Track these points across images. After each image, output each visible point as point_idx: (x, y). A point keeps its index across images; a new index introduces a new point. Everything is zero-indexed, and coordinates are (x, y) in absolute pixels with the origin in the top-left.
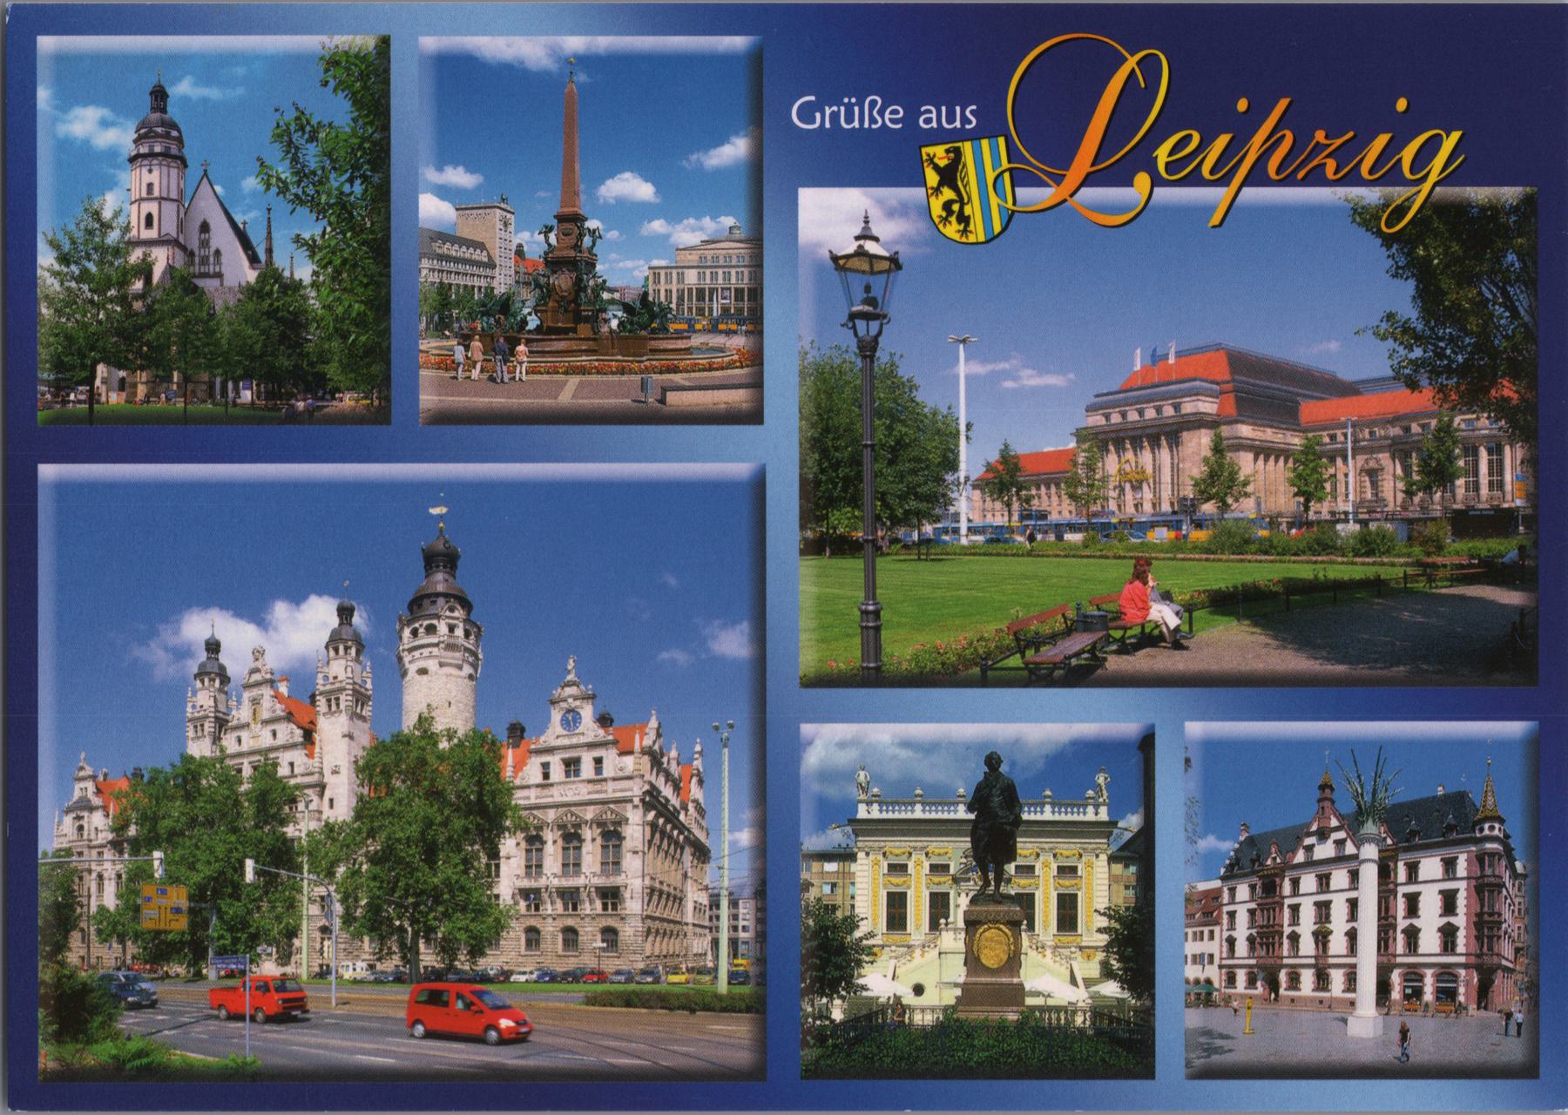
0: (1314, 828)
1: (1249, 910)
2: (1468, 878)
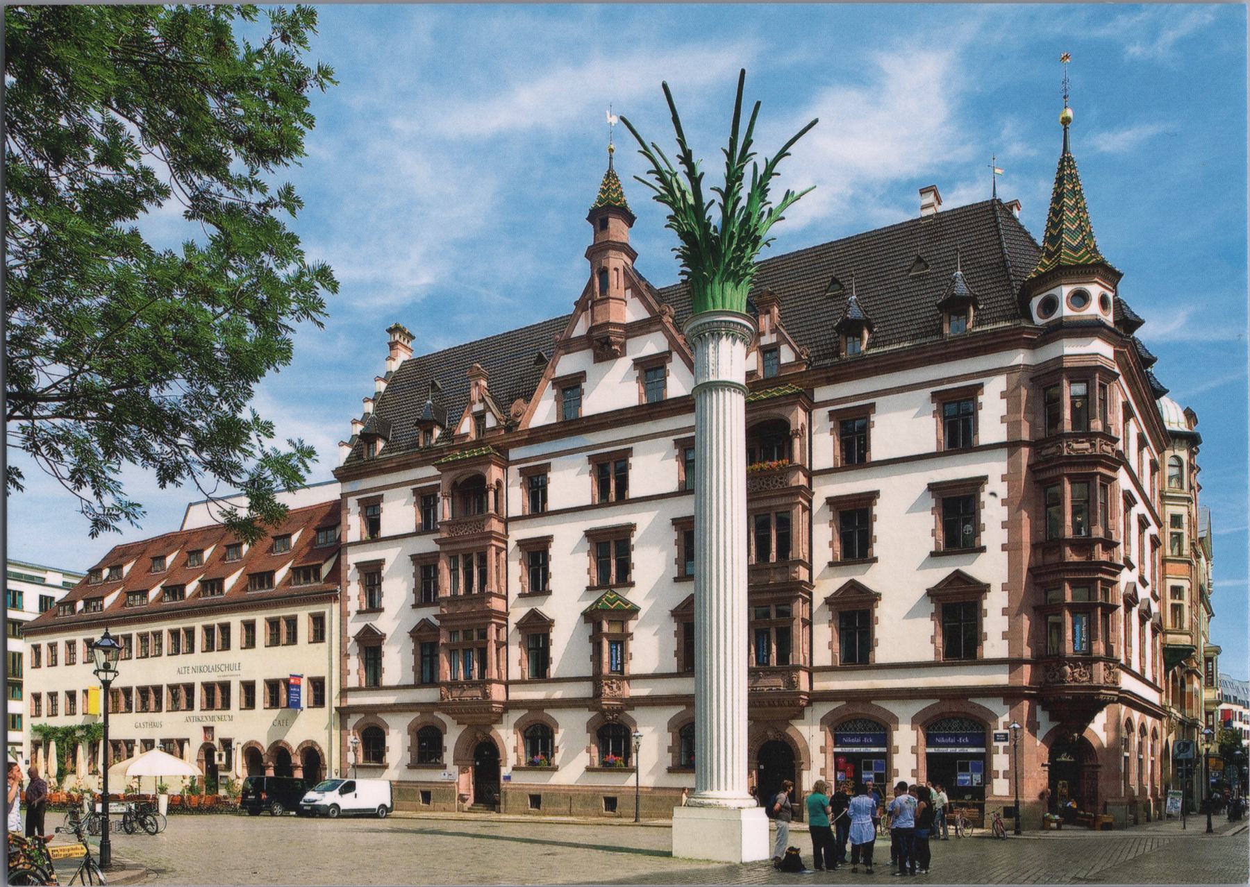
0: (580, 329)
1: (415, 558)
2: (1011, 446)
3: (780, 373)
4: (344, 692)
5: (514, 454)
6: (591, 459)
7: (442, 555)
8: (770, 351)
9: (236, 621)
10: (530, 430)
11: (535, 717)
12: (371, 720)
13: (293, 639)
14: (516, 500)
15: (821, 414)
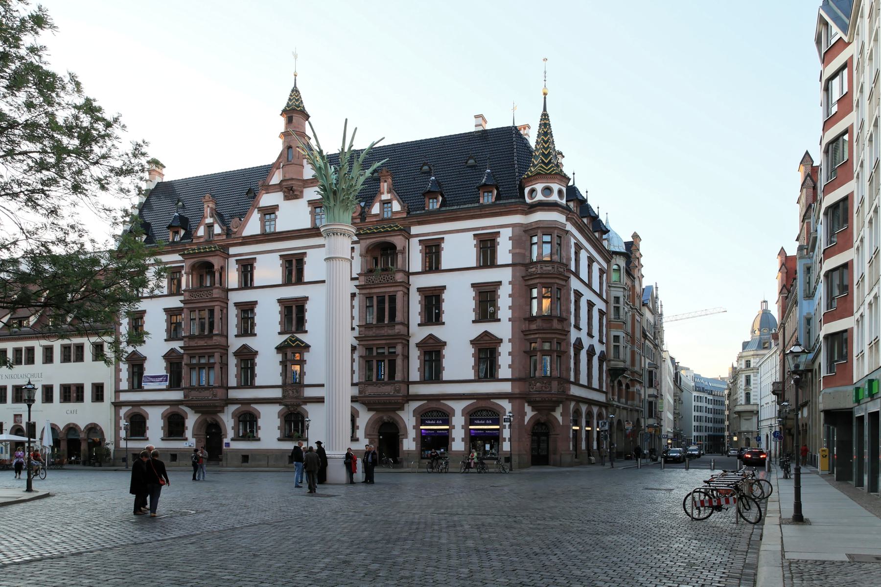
3: (393, 216)
4: (118, 391)
5: (233, 251)
6: (281, 256)
7: (185, 310)
8: (387, 203)
9: (38, 345)
10: (243, 237)
11: (246, 408)
12: (136, 410)
13: (80, 358)
14: (233, 278)
15: (414, 242)
